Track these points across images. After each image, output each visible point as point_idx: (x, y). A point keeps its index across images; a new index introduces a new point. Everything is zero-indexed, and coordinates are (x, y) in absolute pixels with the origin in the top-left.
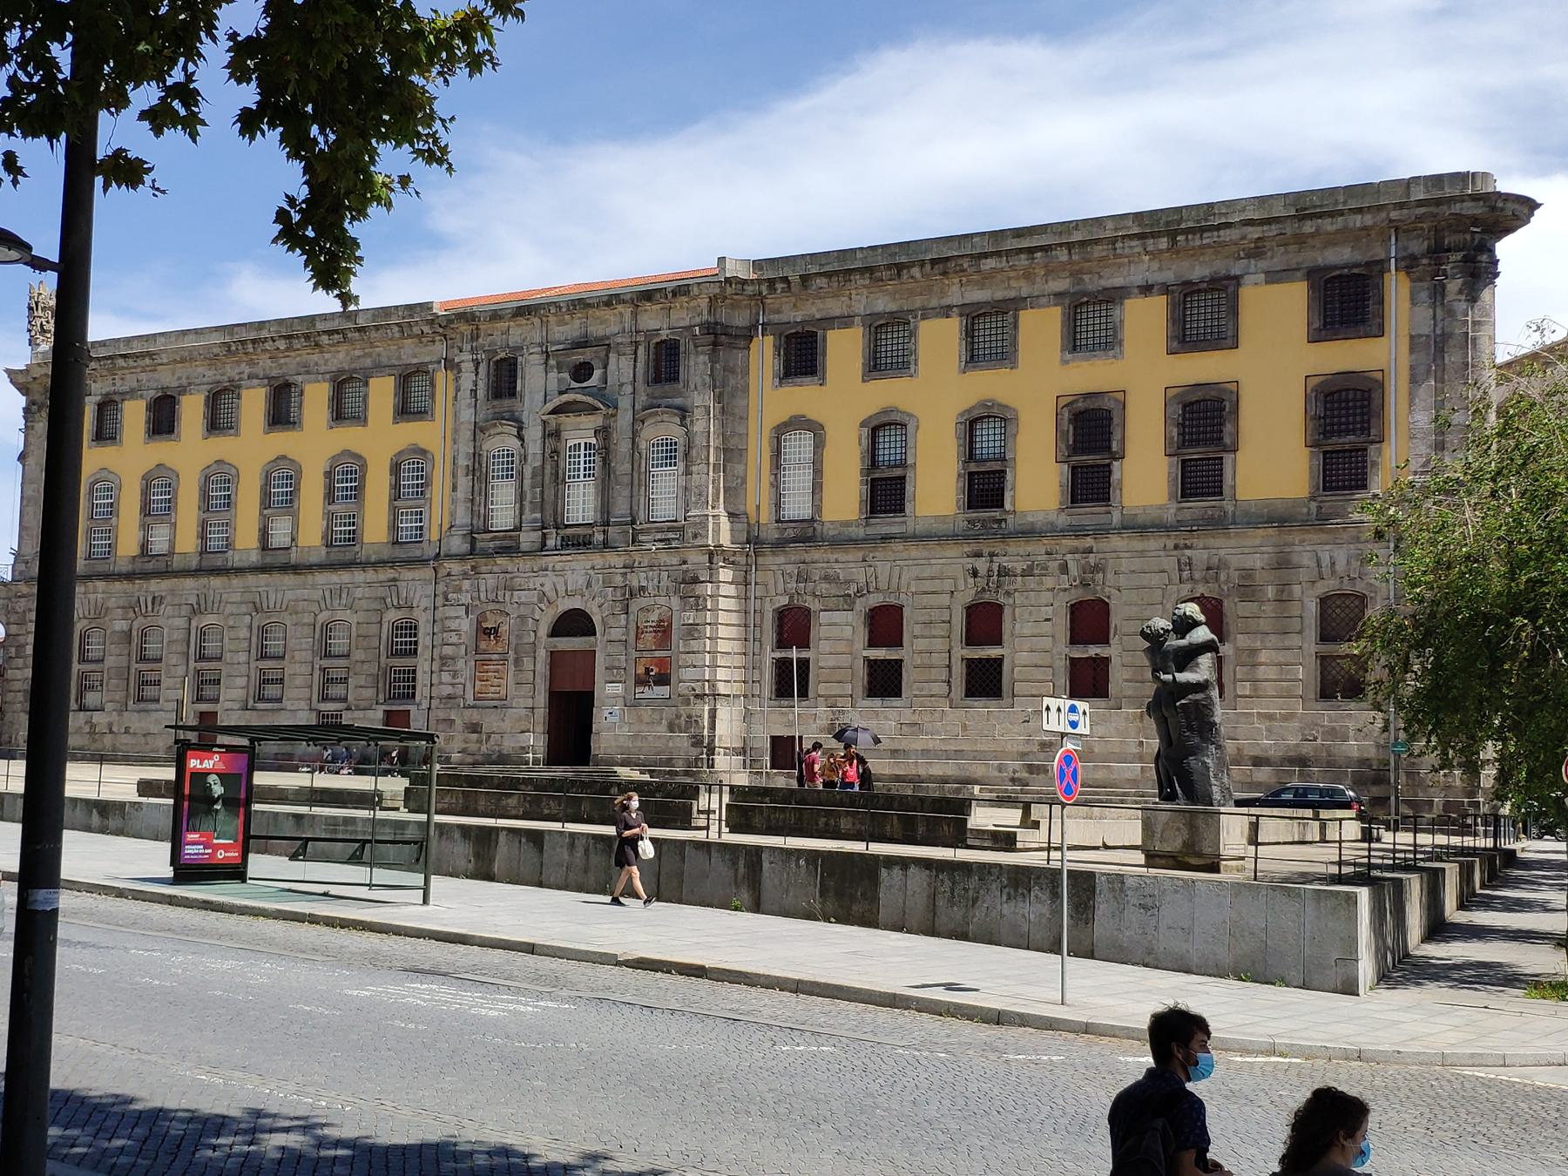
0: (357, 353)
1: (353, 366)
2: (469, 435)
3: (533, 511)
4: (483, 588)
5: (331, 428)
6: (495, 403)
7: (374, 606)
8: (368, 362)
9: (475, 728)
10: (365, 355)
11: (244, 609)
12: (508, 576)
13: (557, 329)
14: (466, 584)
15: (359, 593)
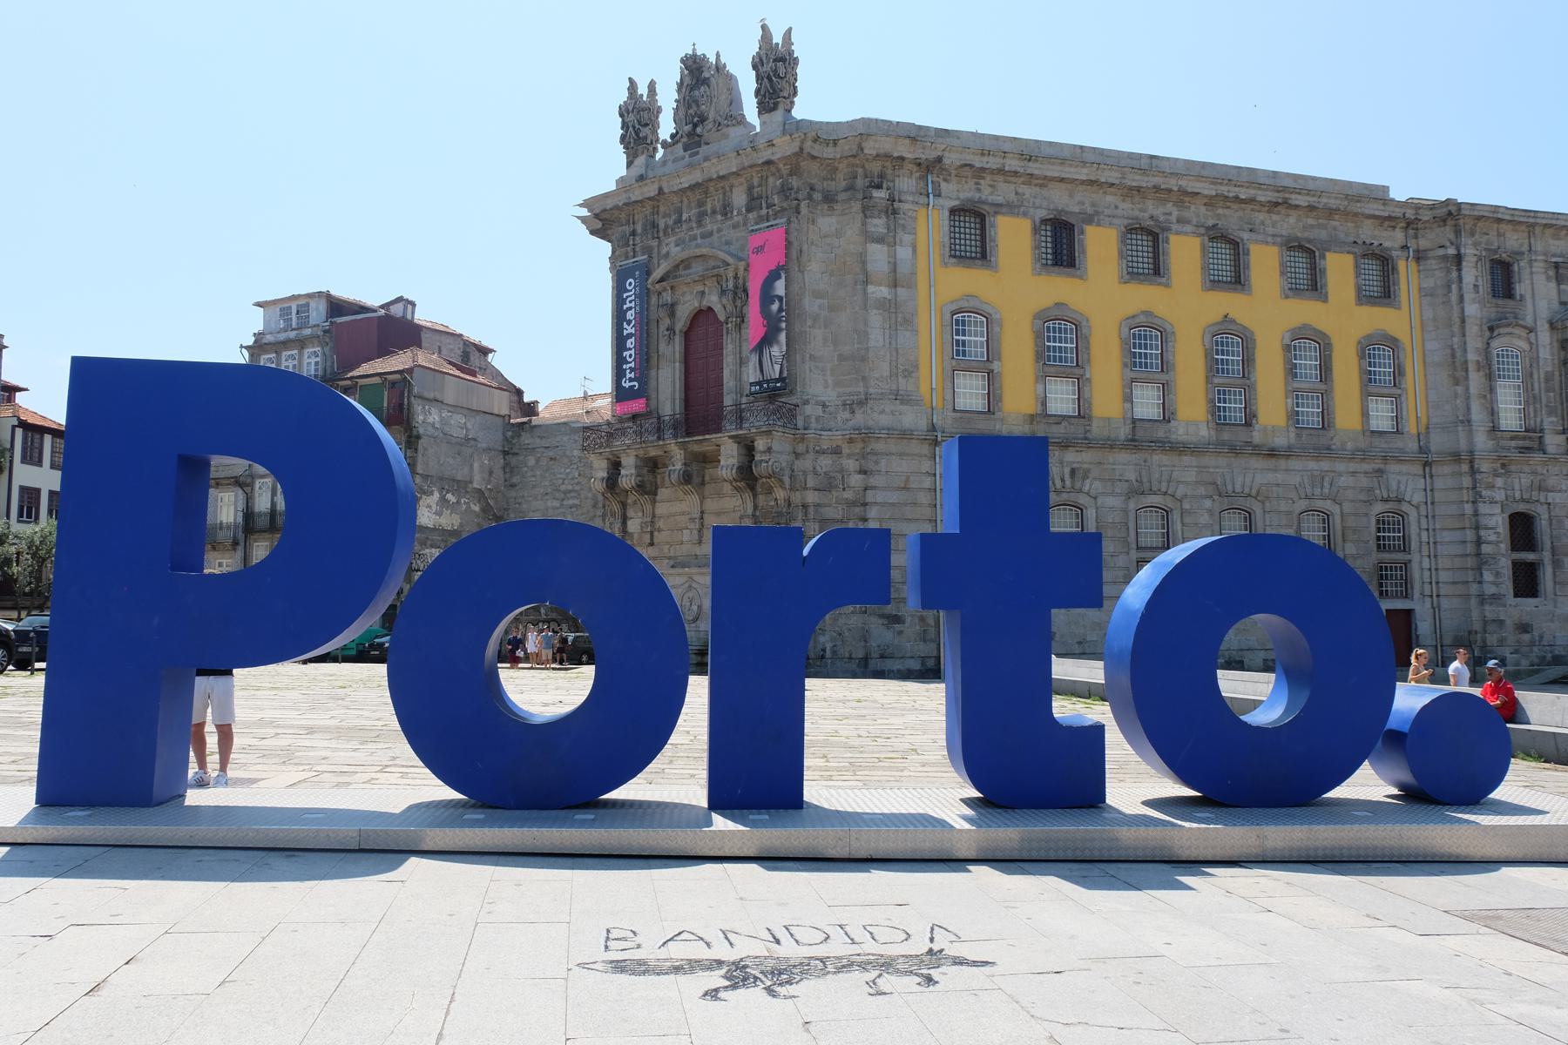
0: (1310, 221)
1: (1306, 234)
2: (1475, 329)
3: (1550, 414)
4: (1517, 487)
5: (1287, 297)
6: (1500, 302)
7: (1362, 497)
8: (1323, 235)
9: (1524, 628)
10: (1319, 226)
11: (1202, 490)
12: (1539, 478)
13: (1551, 242)
14: (1499, 482)
15: (1344, 481)
